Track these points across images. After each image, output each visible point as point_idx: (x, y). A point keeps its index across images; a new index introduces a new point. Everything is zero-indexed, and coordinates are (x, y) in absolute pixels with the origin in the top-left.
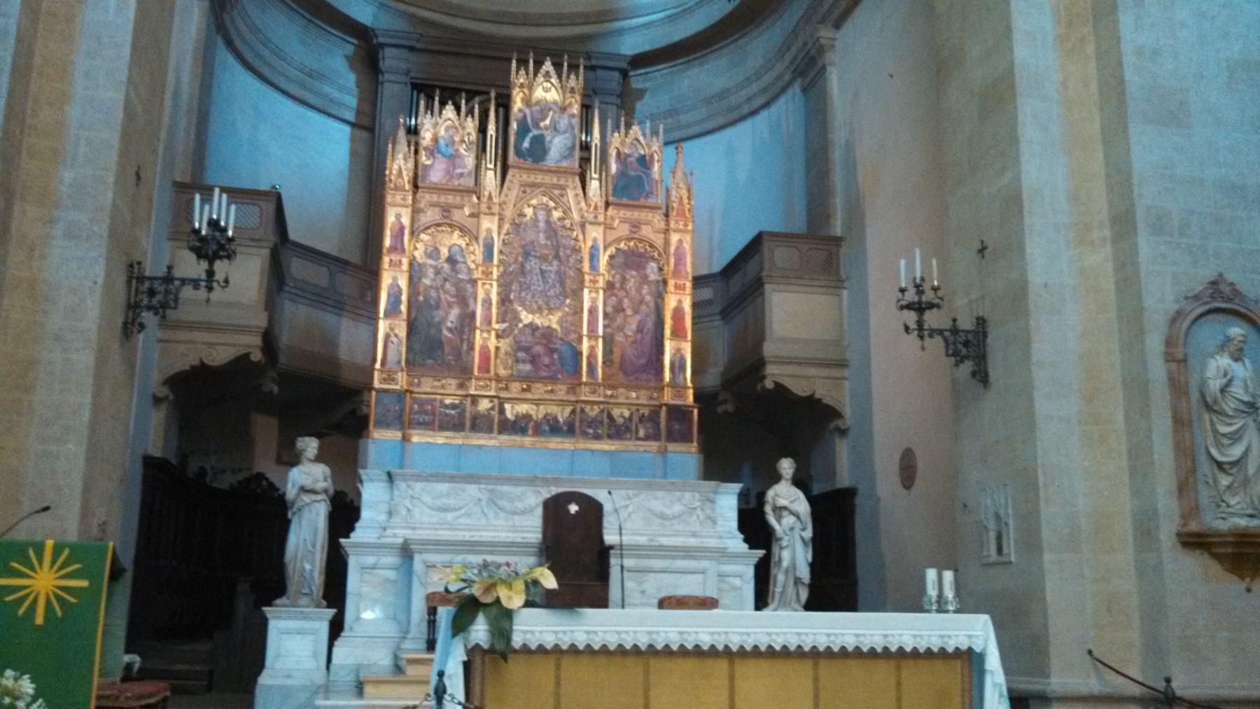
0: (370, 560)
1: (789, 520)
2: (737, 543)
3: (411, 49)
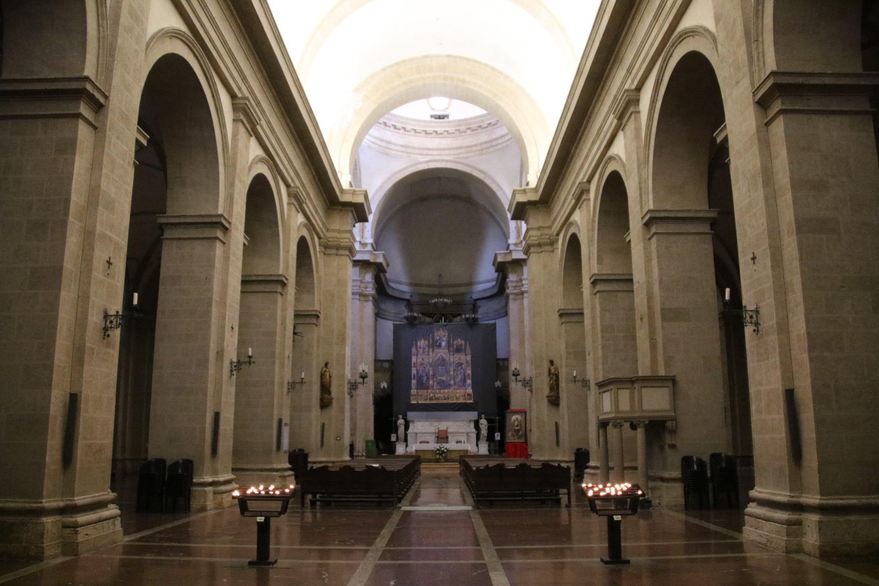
0: (411, 435)
1: (483, 426)
2: (474, 430)
3: (420, 305)
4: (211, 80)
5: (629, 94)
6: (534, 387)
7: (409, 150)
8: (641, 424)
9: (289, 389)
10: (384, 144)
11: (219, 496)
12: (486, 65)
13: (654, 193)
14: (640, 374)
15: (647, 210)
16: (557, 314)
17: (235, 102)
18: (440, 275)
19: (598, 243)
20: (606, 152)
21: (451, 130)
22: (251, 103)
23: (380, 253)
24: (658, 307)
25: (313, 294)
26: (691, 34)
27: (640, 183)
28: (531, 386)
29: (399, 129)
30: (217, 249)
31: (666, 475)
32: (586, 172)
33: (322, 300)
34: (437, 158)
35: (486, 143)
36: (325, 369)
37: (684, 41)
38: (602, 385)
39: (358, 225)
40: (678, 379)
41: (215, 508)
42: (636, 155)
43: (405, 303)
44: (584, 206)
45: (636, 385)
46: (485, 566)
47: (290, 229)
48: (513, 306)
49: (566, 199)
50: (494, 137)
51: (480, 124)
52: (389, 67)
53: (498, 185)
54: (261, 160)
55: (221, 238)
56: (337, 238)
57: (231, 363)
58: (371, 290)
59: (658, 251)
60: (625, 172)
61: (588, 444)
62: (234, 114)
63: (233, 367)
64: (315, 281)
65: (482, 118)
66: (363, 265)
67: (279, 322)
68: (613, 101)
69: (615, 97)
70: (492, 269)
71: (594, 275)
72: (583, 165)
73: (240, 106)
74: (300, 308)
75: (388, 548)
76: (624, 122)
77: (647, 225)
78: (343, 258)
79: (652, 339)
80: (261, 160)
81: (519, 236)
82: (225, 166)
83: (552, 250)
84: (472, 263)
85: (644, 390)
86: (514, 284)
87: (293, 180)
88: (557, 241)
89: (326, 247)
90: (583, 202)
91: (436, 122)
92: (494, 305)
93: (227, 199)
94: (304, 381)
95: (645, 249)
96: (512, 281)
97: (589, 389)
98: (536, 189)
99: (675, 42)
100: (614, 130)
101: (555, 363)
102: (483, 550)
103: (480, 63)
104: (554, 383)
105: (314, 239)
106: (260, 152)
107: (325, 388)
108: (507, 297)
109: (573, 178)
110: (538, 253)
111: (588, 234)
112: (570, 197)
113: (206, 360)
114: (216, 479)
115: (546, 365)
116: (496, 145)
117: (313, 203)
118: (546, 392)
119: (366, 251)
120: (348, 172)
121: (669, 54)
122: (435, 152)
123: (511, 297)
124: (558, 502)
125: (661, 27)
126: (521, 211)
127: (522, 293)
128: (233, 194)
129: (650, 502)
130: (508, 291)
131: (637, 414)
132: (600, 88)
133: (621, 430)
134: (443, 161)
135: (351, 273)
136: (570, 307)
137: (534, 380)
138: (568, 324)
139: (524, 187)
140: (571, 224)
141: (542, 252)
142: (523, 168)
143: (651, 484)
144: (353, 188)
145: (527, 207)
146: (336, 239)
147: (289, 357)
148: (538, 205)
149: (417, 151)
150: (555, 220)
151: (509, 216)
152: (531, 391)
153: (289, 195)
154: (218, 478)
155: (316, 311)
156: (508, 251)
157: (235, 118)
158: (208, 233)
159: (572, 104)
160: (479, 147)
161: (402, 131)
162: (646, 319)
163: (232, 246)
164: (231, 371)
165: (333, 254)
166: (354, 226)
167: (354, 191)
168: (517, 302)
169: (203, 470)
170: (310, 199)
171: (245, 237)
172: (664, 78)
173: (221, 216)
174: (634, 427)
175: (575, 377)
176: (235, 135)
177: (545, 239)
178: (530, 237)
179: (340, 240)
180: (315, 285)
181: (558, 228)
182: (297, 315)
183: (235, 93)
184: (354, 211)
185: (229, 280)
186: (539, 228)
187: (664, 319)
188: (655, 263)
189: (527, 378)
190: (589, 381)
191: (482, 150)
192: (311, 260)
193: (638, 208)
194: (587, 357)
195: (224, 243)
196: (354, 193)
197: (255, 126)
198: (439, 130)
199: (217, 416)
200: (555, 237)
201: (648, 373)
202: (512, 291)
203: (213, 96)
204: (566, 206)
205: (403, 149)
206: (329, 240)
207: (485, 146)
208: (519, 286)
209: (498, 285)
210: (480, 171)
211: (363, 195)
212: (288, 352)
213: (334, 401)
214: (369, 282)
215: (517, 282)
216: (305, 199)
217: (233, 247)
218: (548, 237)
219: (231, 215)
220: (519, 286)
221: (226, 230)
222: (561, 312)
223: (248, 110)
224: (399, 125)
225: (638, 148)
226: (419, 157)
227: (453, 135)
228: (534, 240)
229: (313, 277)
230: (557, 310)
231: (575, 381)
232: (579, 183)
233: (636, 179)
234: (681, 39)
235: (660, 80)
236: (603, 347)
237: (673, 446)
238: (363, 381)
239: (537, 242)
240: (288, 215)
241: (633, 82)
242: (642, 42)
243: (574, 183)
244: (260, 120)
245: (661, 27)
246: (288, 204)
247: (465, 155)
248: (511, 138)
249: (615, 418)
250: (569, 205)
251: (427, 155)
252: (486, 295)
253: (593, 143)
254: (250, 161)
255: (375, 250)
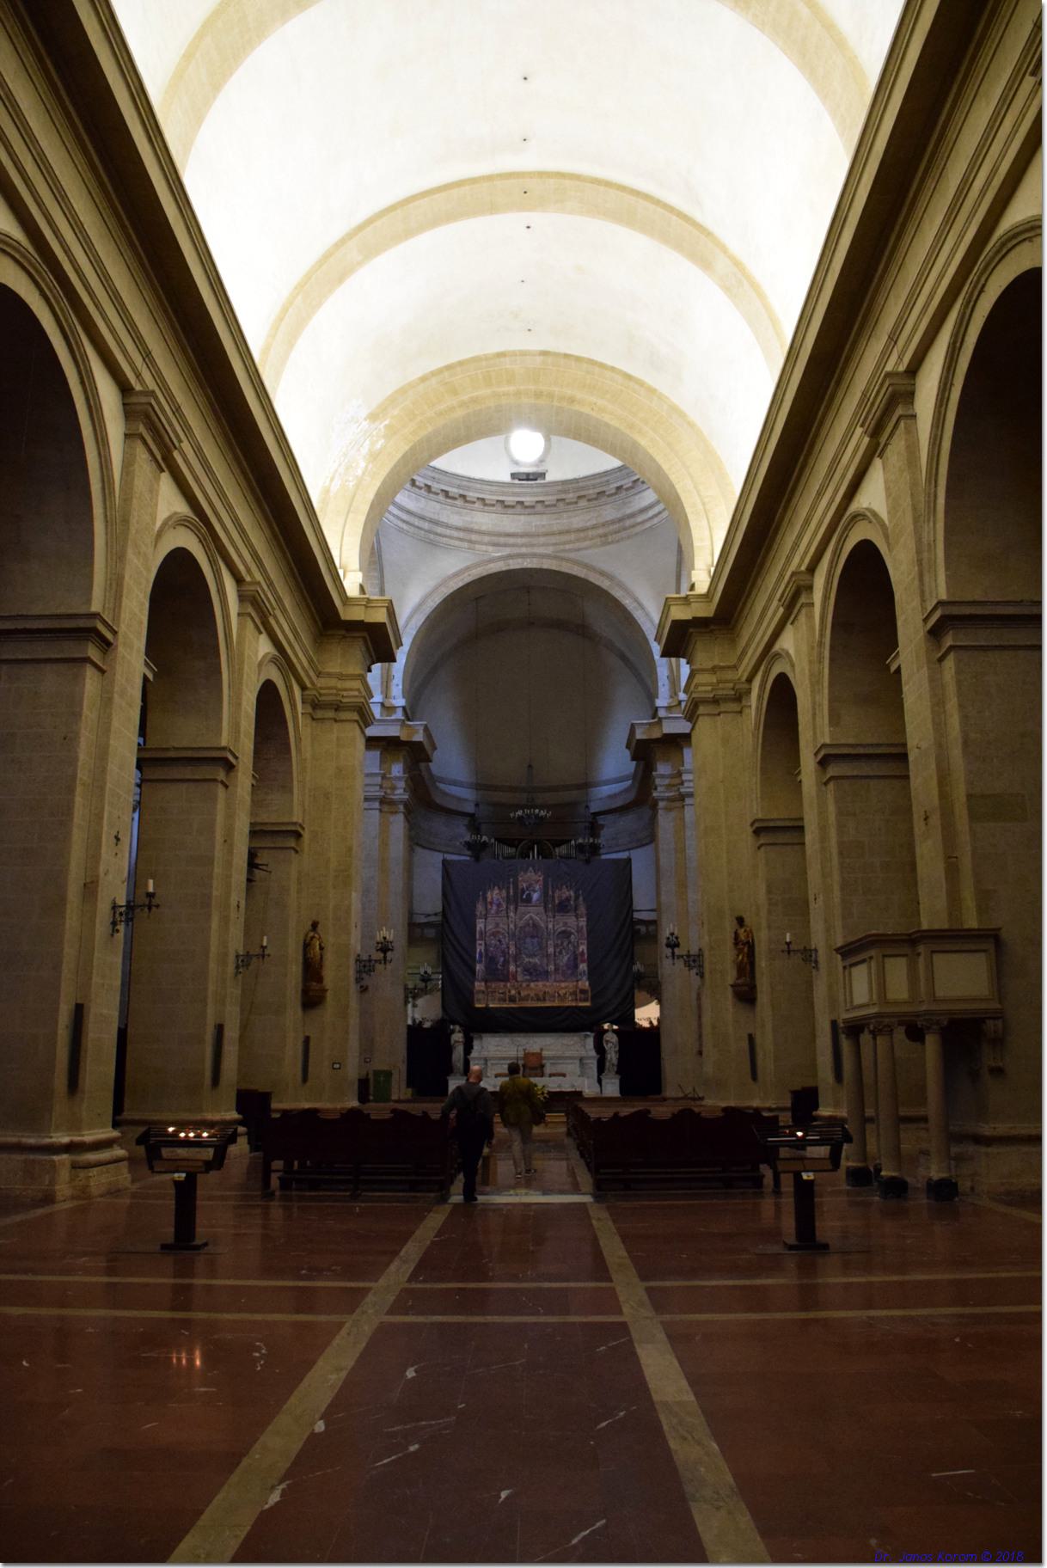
1: (610, 1045)
2: (593, 1053)
4: (80, 352)
5: (896, 380)
6: (707, 966)
7: (474, 537)
8: (935, 1027)
9: (237, 967)
10: (426, 525)
11: (82, 1174)
12: (613, 369)
13: (947, 569)
14: (925, 926)
15: (934, 602)
16: (750, 830)
17: (127, 401)
18: (530, 766)
19: (831, 684)
20: (845, 509)
21: (550, 499)
22: (159, 403)
23: (418, 724)
24: (960, 792)
25: (291, 791)
26: (1027, 235)
27: (919, 552)
28: (701, 966)
29: (455, 499)
30: (88, 682)
31: (986, 1130)
32: (806, 553)
33: (306, 803)
34: (524, 550)
35: (613, 522)
36: (311, 934)
37: (1013, 254)
38: (851, 952)
39: (376, 667)
40: (1004, 935)
41: (73, 1198)
42: (909, 499)
43: (466, 821)
44: (802, 618)
45: (921, 948)
46: (623, 1328)
47: (243, 662)
48: (665, 822)
49: (765, 609)
50: (629, 511)
51: (604, 489)
52: (433, 374)
53: (636, 600)
54: (183, 522)
55: (95, 660)
56: (336, 688)
57: (114, 907)
58: (401, 793)
59: (959, 683)
60: (886, 537)
61: (815, 1076)
62: (126, 424)
63: (117, 915)
64: (294, 767)
65: (606, 479)
66: (386, 746)
67: (219, 838)
68: (859, 405)
69: (864, 395)
70: (627, 754)
71: (824, 746)
72: (800, 536)
73: (139, 408)
74: (264, 817)
75: (414, 1285)
76: (883, 440)
77: (935, 633)
78: (348, 726)
79: (950, 857)
80: (183, 522)
81: (674, 693)
82: (107, 522)
83: (739, 709)
84: (589, 743)
85: (936, 957)
86: (667, 781)
87: (249, 570)
88: (749, 691)
89: (315, 705)
90: (799, 611)
91: (521, 486)
92: (627, 822)
93: (111, 584)
94: (267, 952)
95: (932, 680)
96: (662, 776)
97: (817, 967)
98: (707, 596)
99: (992, 258)
100: (860, 462)
101: (747, 921)
102: (618, 1289)
103: (602, 366)
104: (745, 959)
105: (291, 687)
106: (182, 508)
107: (312, 970)
108: (654, 806)
109: (779, 568)
110: (715, 715)
111: (810, 671)
112: (775, 603)
113: (63, 900)
114: (77, 1139)
115: (729, 926)
116: (633, 526)
117: (290, 618)
118: (731, 976)
119: (393, 721)
120: (357, 566)
121: (980, 286)
122: (519, 541)
123: (661, 804)
124: (758, 1182)
125: (961, 237)
126: (679, 639)
127: (682, 797)
128: (123, 577)
129: (956, 1184)
130: (655, 794)
131: (924, 1007)
132: (833, 384)
133: (892, 1038)
134: (534, 555)
135: (367, 762)
136: (775, 816)
137: (706, 954)
138: (769, 848)
139: (684, 592)
140: (778, 656)
141: (719, 714)
142: (682, 558)
143: (955, 1150)
144: (367, 596)
145: (691, 630)
146: (335, 691)
147: (238, 906)
148: (712, 627)
149: (486, 539)
150: (744, 653)
151: (656, 649)
152: (702, 975)
153: (242, 598)
154: (83, 1136)
155: (295, 824)
156: (656, 720)
157: (127, 432)
158: (70, 649)
159: (778, 419)
160: (601, 531)
161: (459, 502)
162: (935, 820)
163: (118, 677)
164: (114, 923)
165: (331, 719)
166: (370, 671)
167: (369, 600)
168: (673, 814)
169: (51, 1119)
170: (284, 611)
171: (147, 664)
172: (967, 338)
173: (96, 615)
174: (915, 1033)
175: (788, 944)
176: (128, 464)
177: (726, 690)
178: (697, 686)
179: (345, 694)
180: (295, 775)
181: (749, 669)
182: (256, 832)
183: (127, 379)
184: (368, 638)
185: (112, 742)
186: (714, 670)
187: (974, 816)
188: (952, 704)
189: (694, 951)
190: (816, 950)
191: (605, 535)
192: (287, 728)
193: (916, 602)
194: (812, 905)
195: (102, 671)
196: (368, 604)
197: (170, 452)
198: (528, 500)
199: (79, 1012)
200: (746, 686)
201: (942, 923)
202: (662, 795)
203: (82, 383)
204: (765, 624)
205: (461, 535)
206: (322, 692)
207: (612, 528)
208: (674, 786)
209: (637, 785)
210: (603, 574)
211: (385, 610)
212: (238, 895)
213: (329, 995)
214: (399, 779)
215: (671, 777)
216: (273, 609)
217: (120, 678)
218: (731, 685)
219: (116, 617)
220: (674, 786)
221: (106, 645)
222: (757, 825)
223: (155, 418)
224: (453, 491)
225: (914, 484)
226: (490, 548)
227: (554, 509)
228: (704, 691)
229: (290, 759)
230: (750, 821)
231: (789, 952)
232: (793, 574)
233: (912, 545)
234: (1004, 251)
235: (958, 345)
236: (844, 886)
237: (998, 1072)
238: (385, 957)
239: (712, 696)
240: (239, 635)
241: (900, 358)
242: (920, 274)
243: (781, 575)
244: (180, 441)
245: (961, 237)
246: (239, 615)
247: (577, 545)
248: (664, 510)
249: (879, 1015)
250: (772, 619)
251: (505, 545)
252: (614, 806)
253: (820, 494)
254: (158, 524)
255: (409, 720)
